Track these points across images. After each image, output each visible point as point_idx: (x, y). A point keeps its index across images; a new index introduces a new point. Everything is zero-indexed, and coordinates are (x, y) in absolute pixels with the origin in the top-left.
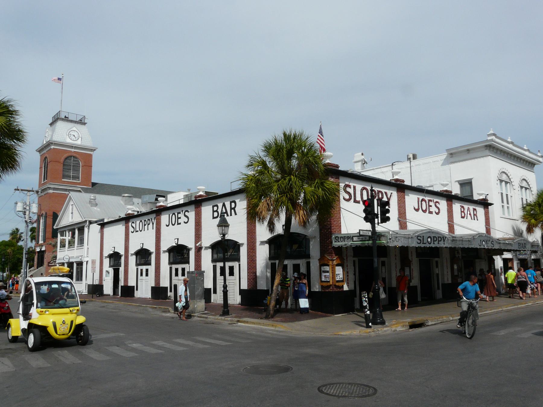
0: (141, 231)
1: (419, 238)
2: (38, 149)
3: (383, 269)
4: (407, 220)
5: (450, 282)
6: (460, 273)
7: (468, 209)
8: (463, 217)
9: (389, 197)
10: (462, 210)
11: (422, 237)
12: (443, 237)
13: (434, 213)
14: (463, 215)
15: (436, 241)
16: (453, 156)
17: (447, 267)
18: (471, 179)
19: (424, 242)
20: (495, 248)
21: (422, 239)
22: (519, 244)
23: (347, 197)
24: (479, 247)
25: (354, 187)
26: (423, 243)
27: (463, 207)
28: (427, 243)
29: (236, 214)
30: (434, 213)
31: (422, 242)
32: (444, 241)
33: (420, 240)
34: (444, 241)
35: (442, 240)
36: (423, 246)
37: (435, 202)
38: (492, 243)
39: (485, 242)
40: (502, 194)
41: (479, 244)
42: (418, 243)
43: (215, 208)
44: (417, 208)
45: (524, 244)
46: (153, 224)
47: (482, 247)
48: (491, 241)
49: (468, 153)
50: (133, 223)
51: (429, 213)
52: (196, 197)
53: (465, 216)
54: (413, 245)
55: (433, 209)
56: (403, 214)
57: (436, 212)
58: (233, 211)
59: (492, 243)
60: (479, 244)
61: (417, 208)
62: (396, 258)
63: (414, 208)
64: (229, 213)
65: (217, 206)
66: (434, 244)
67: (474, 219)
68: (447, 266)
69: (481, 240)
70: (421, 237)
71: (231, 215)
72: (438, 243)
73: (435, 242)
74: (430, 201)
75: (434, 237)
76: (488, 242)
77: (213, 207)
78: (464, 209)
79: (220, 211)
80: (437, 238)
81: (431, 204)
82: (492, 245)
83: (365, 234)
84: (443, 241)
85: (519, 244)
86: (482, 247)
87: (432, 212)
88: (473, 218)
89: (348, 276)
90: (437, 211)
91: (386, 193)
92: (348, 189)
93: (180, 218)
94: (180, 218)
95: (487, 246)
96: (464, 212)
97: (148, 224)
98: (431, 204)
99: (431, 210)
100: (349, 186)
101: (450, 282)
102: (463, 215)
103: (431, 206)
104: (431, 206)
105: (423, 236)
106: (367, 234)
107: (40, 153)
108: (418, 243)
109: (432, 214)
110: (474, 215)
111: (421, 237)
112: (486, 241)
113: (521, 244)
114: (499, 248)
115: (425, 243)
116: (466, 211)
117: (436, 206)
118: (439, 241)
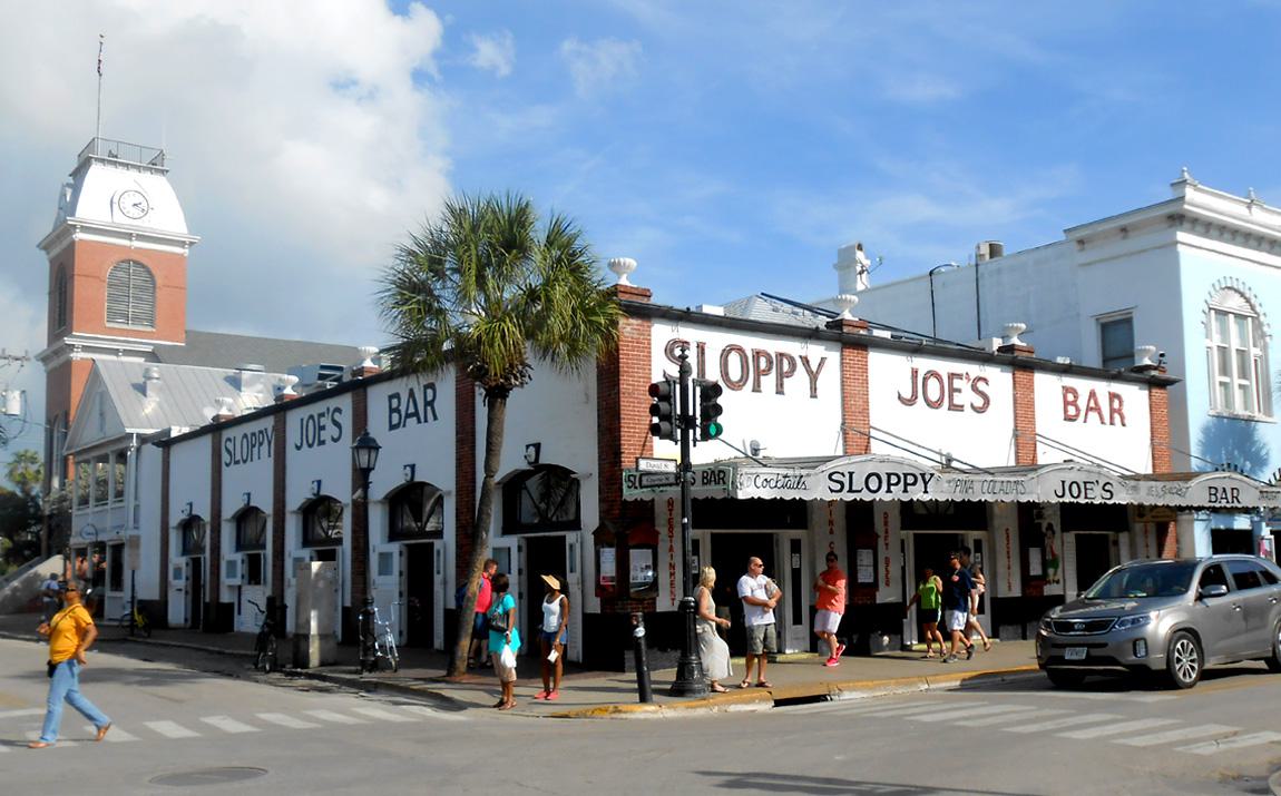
0: (245, 462)
2: (40, 244)
4: (873, 433)
5: (1016, 592)
6: (1051, 571)
7: (1092, 395)
8: (1068, 418)
9: (814, 368)
10: (1070, 397)
12: (923, 475)
13: (968, 408)
14: (1072, 411)
15: (897, 484)
16: (1086, 245)
17: (1008, 552)
18: (1129, 312)
19: (854, 488)
21: (846, 481)
24: (1054, 500)
25: (701, 348)
26: (851, 491)
27: (1074, 392)
29: (435, 418)
30: (968, 408)
32: (926, 483)
34: (926, 483)
36: (850, 497)
38: (1106, 488)
40: (1223, 351)
42: (832, 491)
43: (395, 402)
44: (907, 394)
46: (269, 443)
47: (1067, 501)
48: (1101, 484)
49: (1124, 238)
50: (229, 440)
51: (949, 409)
52: (355, 373)
53: (1077, 415)
55: (966, 397)
57: (976, 405)
58: (429, 408)
59: (1106, 488)
61: (907, 394)
64: (422, 419)
65: (397, 396)
66: (889, 491)
67: (1112, 423)
68: (1008, 552)
69: (1063, 482)
71: (426, 421)
72: (905, 491)
73: (892, 488)
74: (952, 376)
75: (889, 475)
76: (1088, 486)
77: (391, 397)
79: (403, 409)
80: (902, 476)
81: (957, 383)
82: (1108, 495)
83: (656, 469)
84: (923, 485)
86: (1067, 499)
87: (962, 406)
88: (1107, 419)
90: (979, 402)
91: (806, 361)
93: (323, 428)
94: (323, 428)
95: (1086, 498)
96: (1074, 403)
97: (261, 444)
98: (957, 383)
99: (958, 399)
101: (1016, 592)
102: (1072, 411)
103: (959, 391)
104: (959, 391)
105: (851, 474)
106: (663, 469)
107: (48, 253)
108: (832, 491)
110: (1112, 411)
111: (843, 474)
112: (1085, 483)
113: (1220, 491)
115: (860, 491)
116: (1082, 403)
117: (974, 388)
118: (906, 484)
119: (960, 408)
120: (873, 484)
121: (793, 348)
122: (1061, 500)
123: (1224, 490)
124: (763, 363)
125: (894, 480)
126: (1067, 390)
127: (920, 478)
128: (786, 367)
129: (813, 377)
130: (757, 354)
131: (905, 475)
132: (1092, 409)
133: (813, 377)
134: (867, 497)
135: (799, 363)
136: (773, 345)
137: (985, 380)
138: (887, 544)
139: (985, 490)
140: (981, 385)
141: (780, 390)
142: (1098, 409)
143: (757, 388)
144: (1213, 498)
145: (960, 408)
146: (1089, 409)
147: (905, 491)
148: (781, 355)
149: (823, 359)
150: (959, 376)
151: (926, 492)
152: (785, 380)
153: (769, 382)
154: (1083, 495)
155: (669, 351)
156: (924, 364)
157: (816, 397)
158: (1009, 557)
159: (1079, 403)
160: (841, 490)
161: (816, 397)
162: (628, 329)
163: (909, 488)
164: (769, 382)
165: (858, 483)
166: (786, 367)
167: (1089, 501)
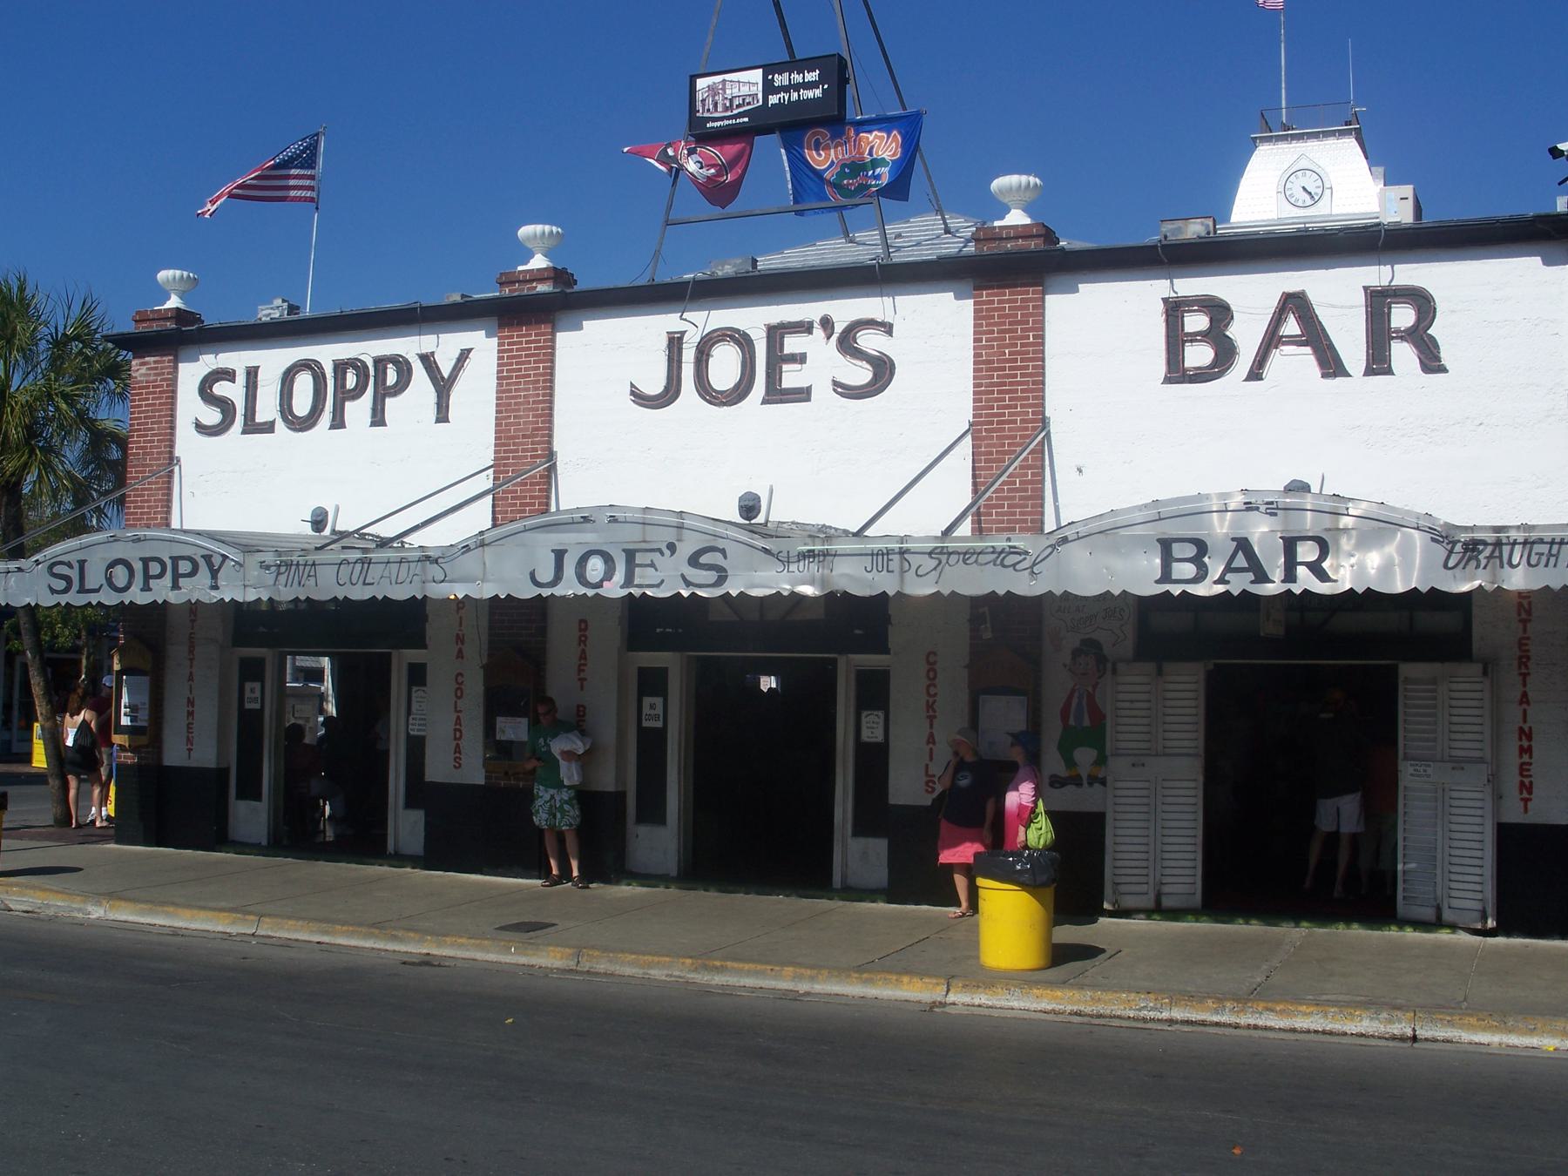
1: (58, 569)
3: (414, 699)
7: (1295, 304)
8: (1177, 373)
10: (1196, 322)
11: (76, 566)
13: (823, 393)
14: (1199, 355)
15: (160, 576)
19: (87, 588)
20: (734, 593)
21: (74, 574)
23: (212, 416)
24: (527, 592)
25: (252, 373)
26: (82, 590)
28: (106, 587)
30: (823, 393)
31: (76, 586)
32: (214, 574)
33: (68, 579)
34: (214, 574)
35: (204, 570)
37: (839, 328)
38: (703, 559)
39: (608, 559)
41: (532, 576)
42: (53, 591)
44: (654, 384)
45: (1290, 545)
48: (686, 549)
54: (27, 600)
56: (524, 436)
60: (532, 576)
62: (460, 651)
63: (640, 398)
66: (146, 588)
68: (930, 707)
69: (560, 555)
70: (70, 565)
72: (175, 586)
75: (146, 562)
76: (639, 558)
78: (1219, 312)
81: (792, 344)
82: (711, 576)
85: (1179, 550)
86: (569, 588)
89: (191, 714)
90: (860, 374)
91: (427, 360)
92: (221, 389)
98: (792, 344)
99: (791, 377)
100: (228, 375)
103: (800, 359)
104: (800, 359)
105: (82, 563)
108: (53, 591)
109: (808, 399)
111: (70, 565)
114: (808, 590)
115: (97, 591)
117: (847, 344)
118: (176, 576)
119: (803, 395)
120: (120, 575)
121: (408, 346)
122: (546, 592)
123: (1243, 545)
124: (351, 380)
125: (155, 568)
126: (1175, 309)
127: (202, 562)
128: (392, 377)
129: (443, 387)
130: (341, 367)
131: (175, 560)
132: (1293, 341)
133: (443, 387)
134: (109, 598)
135: (419, 370)
136: (368, 349)
137: (888, 328)
138: (582, 680)
139: (344, 578)
140: (869, 341)
141: (378, 419)
142: (1316, 338)
143: (338, 422)
144: (1187, 570)
145: (803, 395)
146: (1272, 340)
147: (176, 586)
148: (380, 362)
149: (464, 355)
150: (805, 328)
151: (215, 587)
152: (388, 401)
153: (360, 410)
154: (619, 576)
155: (205, 390)
156: (699, 321)
157: (446, 420)
158: (931, 719)
159: (1233, 332)
160: (66, 591)
161: (446, 420)
162: (143, 370)
163: (182, 581)
164: (360, 410)
165: (95, 578)
166: (392, 377)
167: (636, 592)
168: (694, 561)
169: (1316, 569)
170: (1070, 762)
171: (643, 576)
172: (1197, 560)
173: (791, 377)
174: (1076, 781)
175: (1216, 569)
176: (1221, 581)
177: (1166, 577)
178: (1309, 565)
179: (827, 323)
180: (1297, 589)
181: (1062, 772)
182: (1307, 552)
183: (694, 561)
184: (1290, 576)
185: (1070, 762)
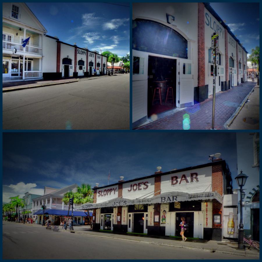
22: (163, 198)
39: (118, 203)
45: (173, 197)
68: (151, 217)
69: (115, 203)
76: (120, 202)
82: (125, 204)
101: (153, 225)
119: (141, 189)
123: (169, 198)
141: (110, 194)
143: (107, 195)
144: (163, 200)
145: (141, 189)
154: (119, 204)
168: (124, 203)
169: (176, 199)
170: (163, 222)
171: (120, 204)
172: (165, 199)
173: (140, 188)
174: (163, 223)
175: (166, 201)
176: (167, 201)
177: (162, 201)
178: (175, 199)
179: (143, 182)
180: (174, 202)
181: (162, 223)
182: (175, 198)
183: (124, 203)
184: (173, 200)
185: (163, 222)
